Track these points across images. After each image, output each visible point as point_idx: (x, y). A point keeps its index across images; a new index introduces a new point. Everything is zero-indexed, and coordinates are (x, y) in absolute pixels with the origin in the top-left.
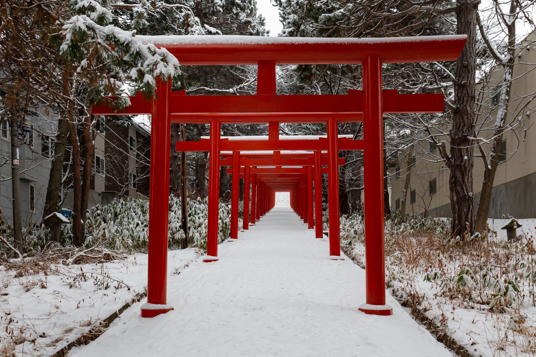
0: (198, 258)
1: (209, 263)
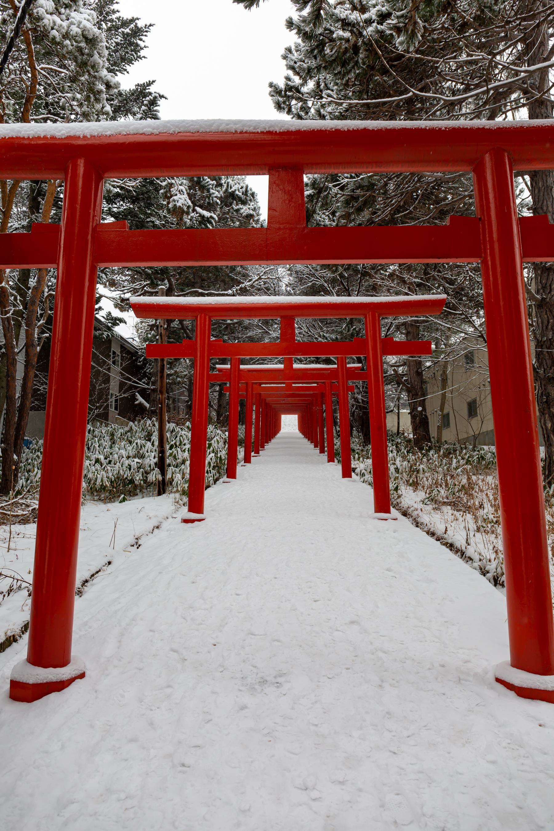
1: (190, 525)
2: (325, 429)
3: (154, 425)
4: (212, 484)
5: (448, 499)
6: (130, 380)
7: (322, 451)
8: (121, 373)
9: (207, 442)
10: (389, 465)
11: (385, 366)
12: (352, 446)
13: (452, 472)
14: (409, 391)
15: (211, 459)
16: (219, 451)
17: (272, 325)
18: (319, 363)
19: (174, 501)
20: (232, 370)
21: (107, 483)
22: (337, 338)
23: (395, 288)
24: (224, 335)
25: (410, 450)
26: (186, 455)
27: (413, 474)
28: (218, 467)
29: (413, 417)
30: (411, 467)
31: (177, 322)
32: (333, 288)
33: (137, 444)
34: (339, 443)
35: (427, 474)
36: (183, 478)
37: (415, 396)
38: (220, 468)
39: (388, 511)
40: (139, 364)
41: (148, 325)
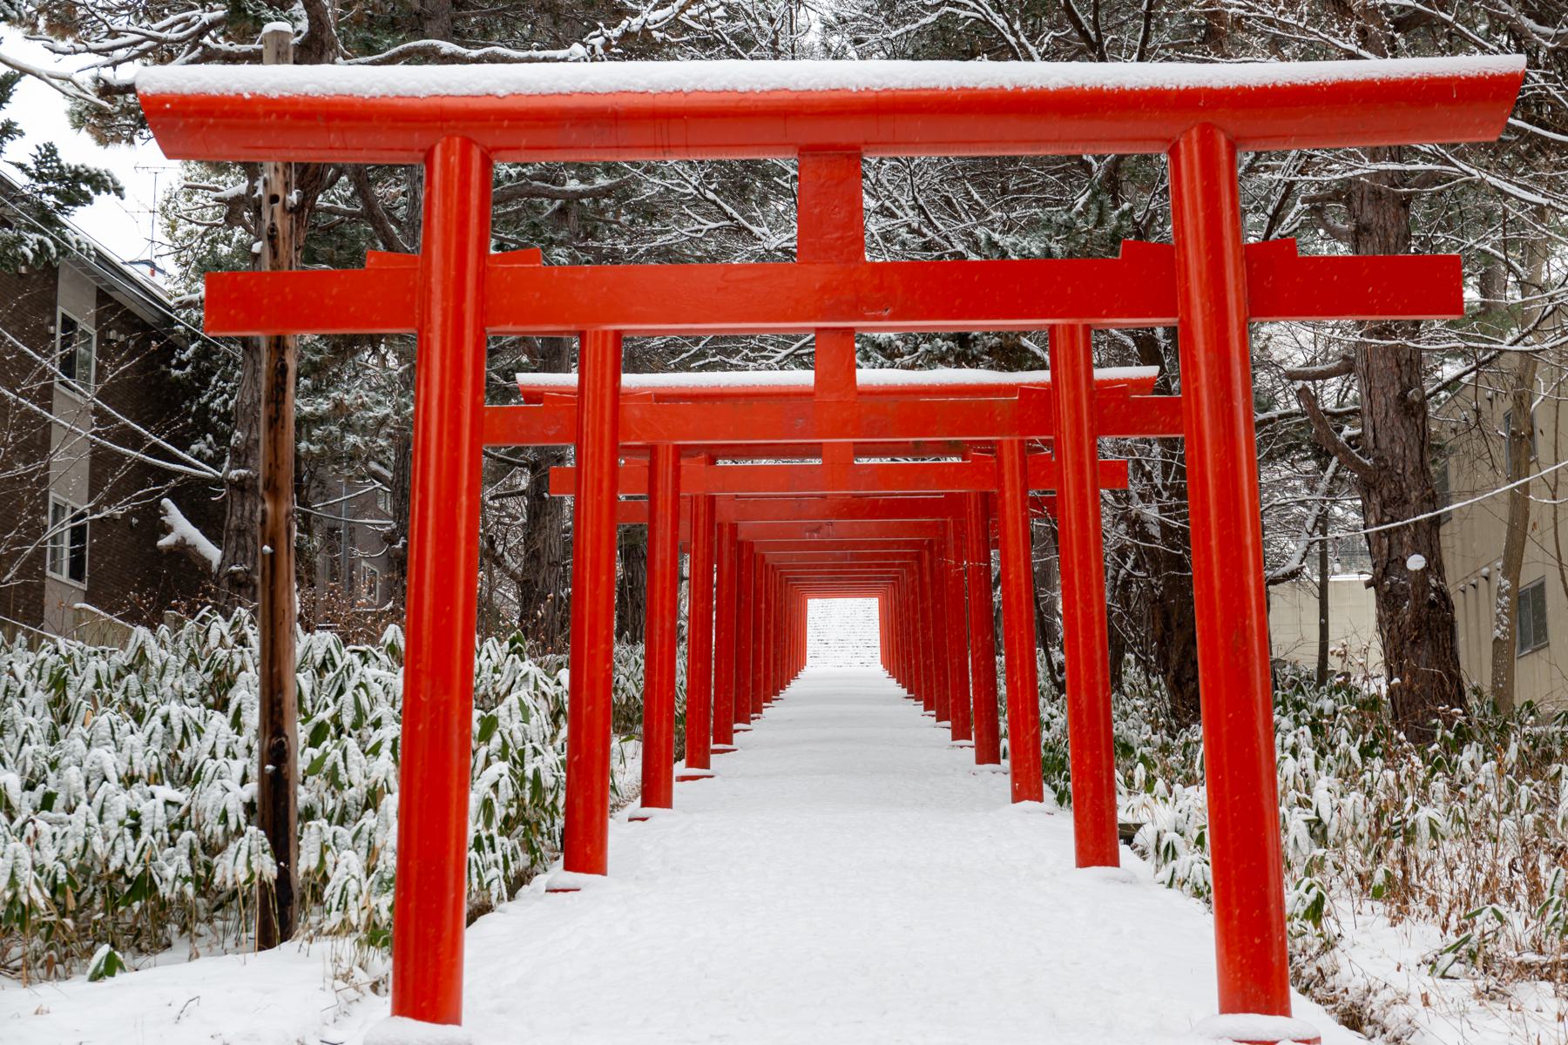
0: (343, 1013)
2: (1000, 660)
3: (242, 641)
4: (500, 899)
5: (1541, 952)
6: (136, 441)
7: (989, 754)
8: (97, 411)
9: (476, 714)
10: (1283, 809)
11: (1263, 378)
12: (1120, 728)
13: (1556, 834)
14: (1367, 487)
15: (495, 786)
16: (529, 752)
17: (763, 201)
18: (973, 362)
19: (330, 970)
20: (588, 394)
21: (35, 893)
22: (1048, 252)
23: (1303, 31)
24: (551, 242)
25: (1373, 744)
26: (385, 767)
27: (1388, 846)
28: (526, 823)
29: (1388, 601)
30: (1379, 815)
31: (344, 187)
32: (1032, 38)
33: (166, 720)
34: (1061, 720)
35: (1449, 849)
36: (370, 870)
37: (1396, 503)
38: (532, 827)
39: (1285, 1012)
40: (176, 373)
41: (216, 199)
